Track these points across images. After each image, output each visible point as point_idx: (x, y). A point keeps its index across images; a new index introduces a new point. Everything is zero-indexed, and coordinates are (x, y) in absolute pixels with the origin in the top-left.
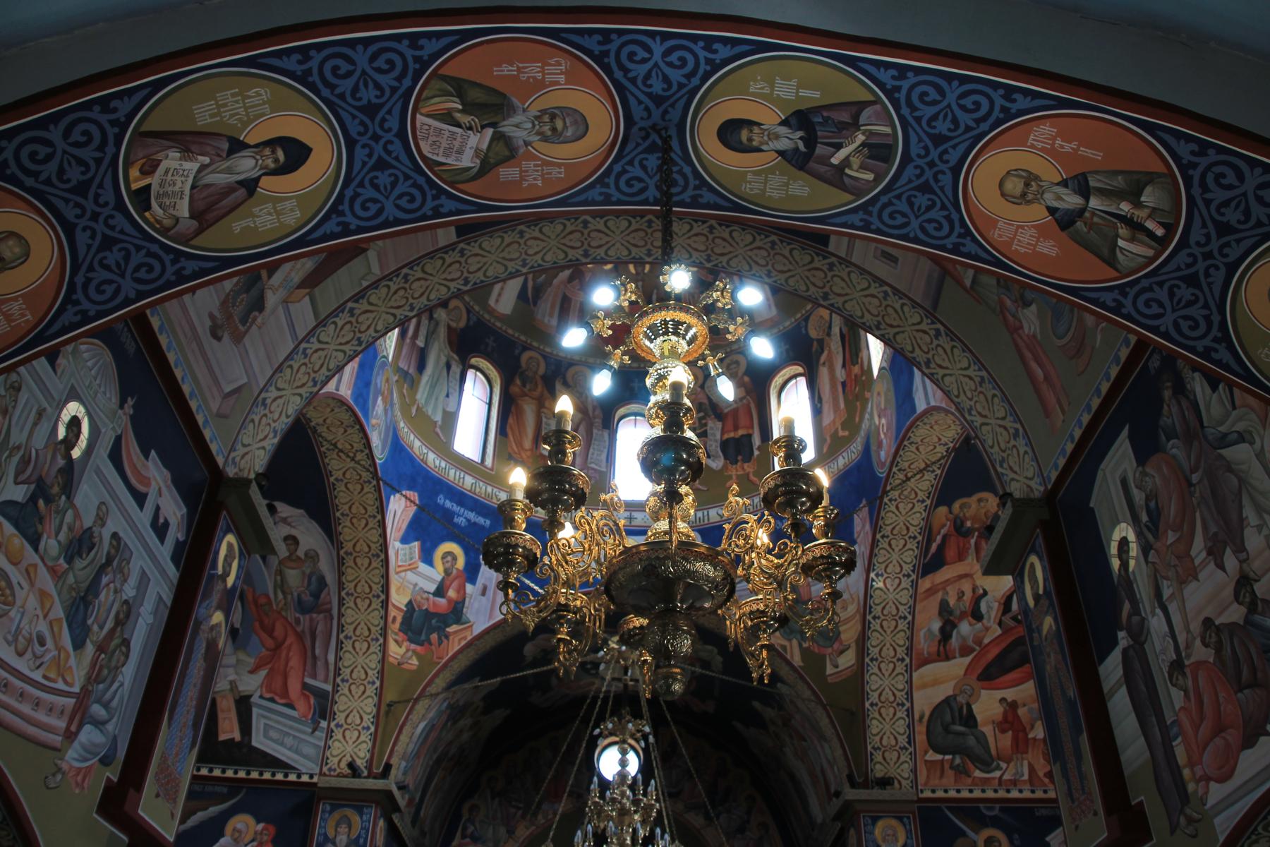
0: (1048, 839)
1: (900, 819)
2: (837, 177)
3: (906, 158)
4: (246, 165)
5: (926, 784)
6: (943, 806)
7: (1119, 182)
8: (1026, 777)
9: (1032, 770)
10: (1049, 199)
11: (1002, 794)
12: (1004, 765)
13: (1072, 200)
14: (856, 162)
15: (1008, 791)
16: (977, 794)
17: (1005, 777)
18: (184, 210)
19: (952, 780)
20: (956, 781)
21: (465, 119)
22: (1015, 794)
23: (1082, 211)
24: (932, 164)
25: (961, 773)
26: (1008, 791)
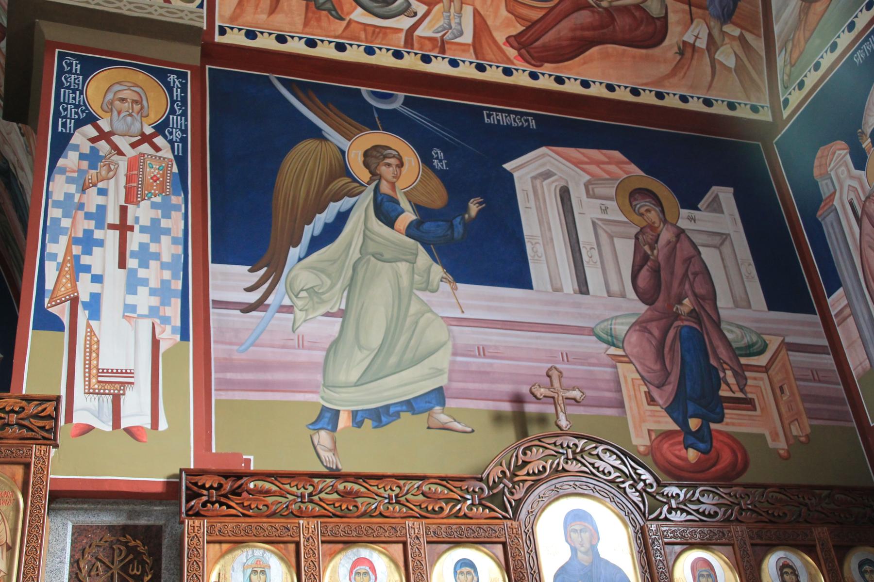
0: (508, 166)
1: (161, 75)
5: (233, 18)
6: (273, 77)
8: (468, 38)
9: (481, 27)
11: (411, 62)
12: (421, 9)
15: (426, 59)
16: (354, 55)
17: (419, 32)
19: (299, 20)
20: (306, 24)
22: (439, 67)
25: (319, 8)
26: (426, 59)
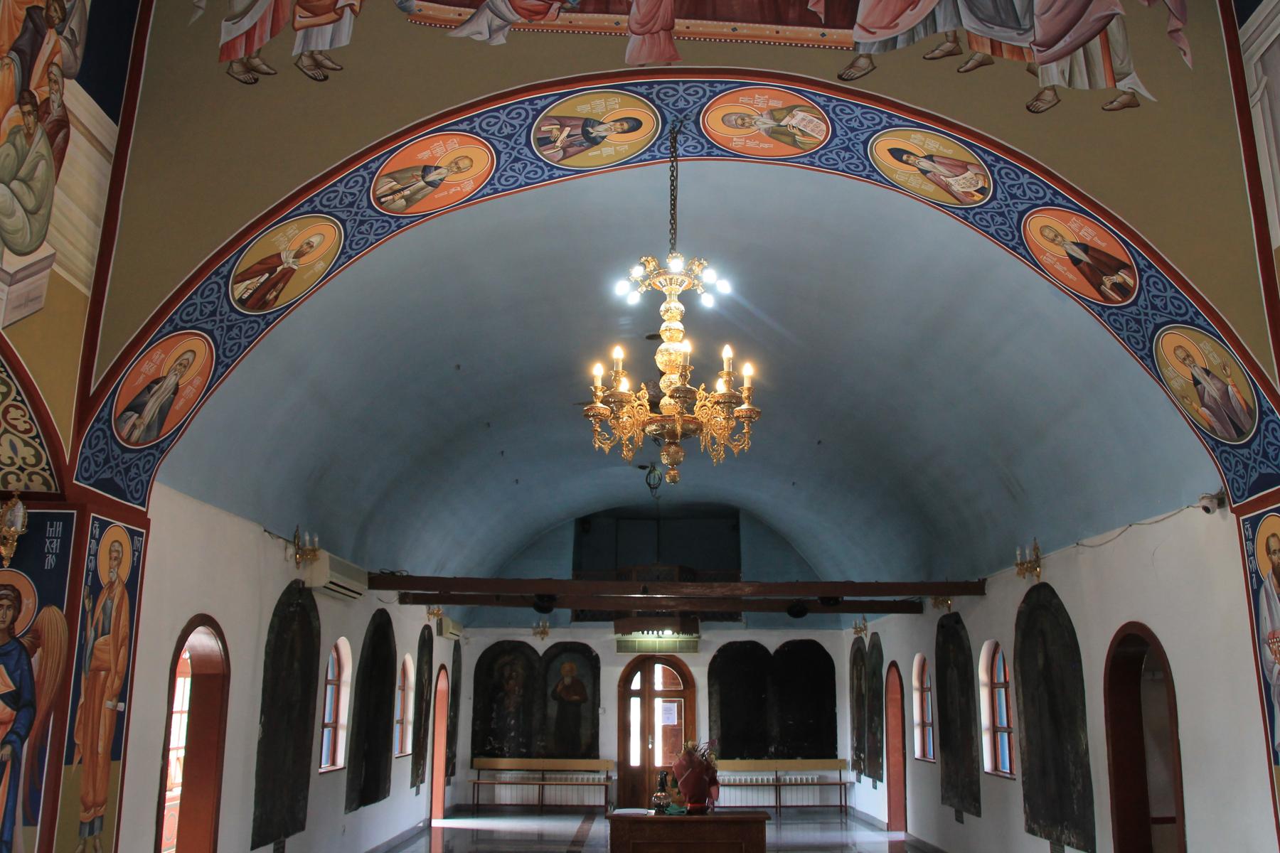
2: (562, 122)
3: (528, 144)
4: (926, 164)
7: (419, 196)
10: (443, 171)
13: (432, 177)
14: (556, 133)
18: (968, 174)
21: (795, 131)
23: (423, 177)
24: (513, 149)
